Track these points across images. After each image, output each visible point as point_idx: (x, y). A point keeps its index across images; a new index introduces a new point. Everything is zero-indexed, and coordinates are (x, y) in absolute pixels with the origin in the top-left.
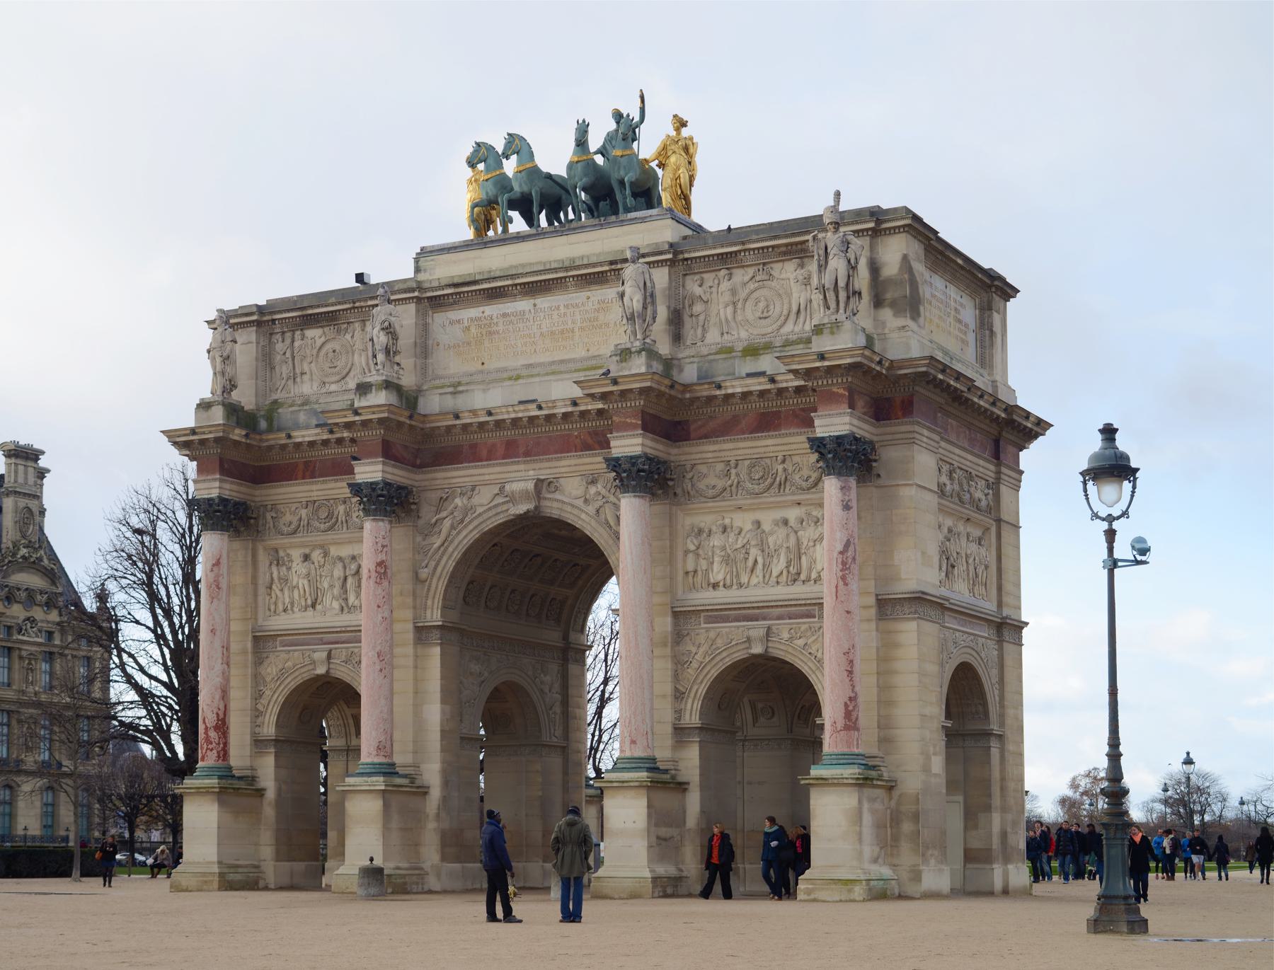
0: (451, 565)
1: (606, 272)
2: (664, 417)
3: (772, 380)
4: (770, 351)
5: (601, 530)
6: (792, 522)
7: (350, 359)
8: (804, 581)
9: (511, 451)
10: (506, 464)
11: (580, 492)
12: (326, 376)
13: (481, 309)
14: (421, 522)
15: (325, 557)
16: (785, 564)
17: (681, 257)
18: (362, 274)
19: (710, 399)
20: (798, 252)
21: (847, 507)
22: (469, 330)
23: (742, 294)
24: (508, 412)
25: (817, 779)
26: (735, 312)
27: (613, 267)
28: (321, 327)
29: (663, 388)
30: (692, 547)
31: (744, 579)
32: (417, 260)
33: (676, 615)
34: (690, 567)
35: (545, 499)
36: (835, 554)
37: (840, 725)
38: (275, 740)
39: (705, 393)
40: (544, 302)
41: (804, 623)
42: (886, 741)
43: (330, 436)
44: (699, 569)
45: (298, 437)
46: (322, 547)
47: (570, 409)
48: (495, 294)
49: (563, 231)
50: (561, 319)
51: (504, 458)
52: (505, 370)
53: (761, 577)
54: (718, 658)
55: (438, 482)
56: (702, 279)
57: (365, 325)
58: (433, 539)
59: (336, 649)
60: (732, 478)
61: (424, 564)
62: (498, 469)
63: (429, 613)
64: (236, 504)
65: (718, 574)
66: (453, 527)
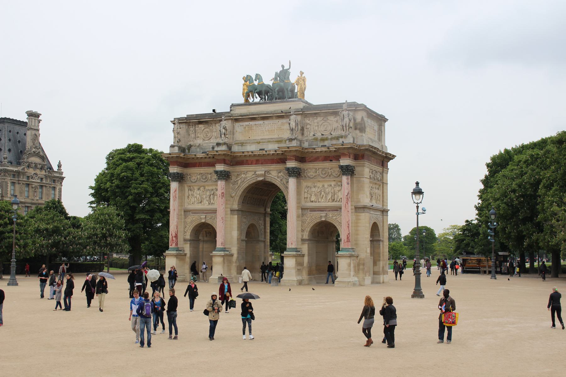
0: (240, 193)
1: (284, 115)
2: (300, 156)
3: (328, 148)
5: (282, 185)
6: (332, 186)
9: (257, 162)
10: (256, 166)
11: (276, 175)
12: (205, 138)
13: (249, 122)
14: (232, 181)
17: (304, 113)
18: (215, 110)
19: (312, 152)
20: (335, 114)
21: (348, 184)
23: (320, 123)
24: (257, 153)
25: (340, 255)
26: (318, 128)
27: (286, 114)
28: (204, 124)
29: (300, 150)
30: (306, 191)
32: (231, 107)
33: (302, 209)
34: (306, 197)
35: (267, 176)
36: (345, 196)
37: (346, 241)
38: (190, 240)
39: (311, 151)
40: (266, 122)
42: (356, 244)
43: (207, 156)
44: (308, 197)
45: (198, 156)
46: (203, 186)
47: (274, 153)
48: (253, 119)
49: (271, 103)
51: (256, 164)
52: (256, 140)
53: (324, 199)
54: (313, 221)
55: (237, 170)
56: (309, 119)
57: (216, 125)
58: (236, 186)
59: (208, 215)
60: (317, 173)
61: (233, 193)
63: (234, 206)
64: (181, 174)
65: (313, 198)
66: (241, 183)
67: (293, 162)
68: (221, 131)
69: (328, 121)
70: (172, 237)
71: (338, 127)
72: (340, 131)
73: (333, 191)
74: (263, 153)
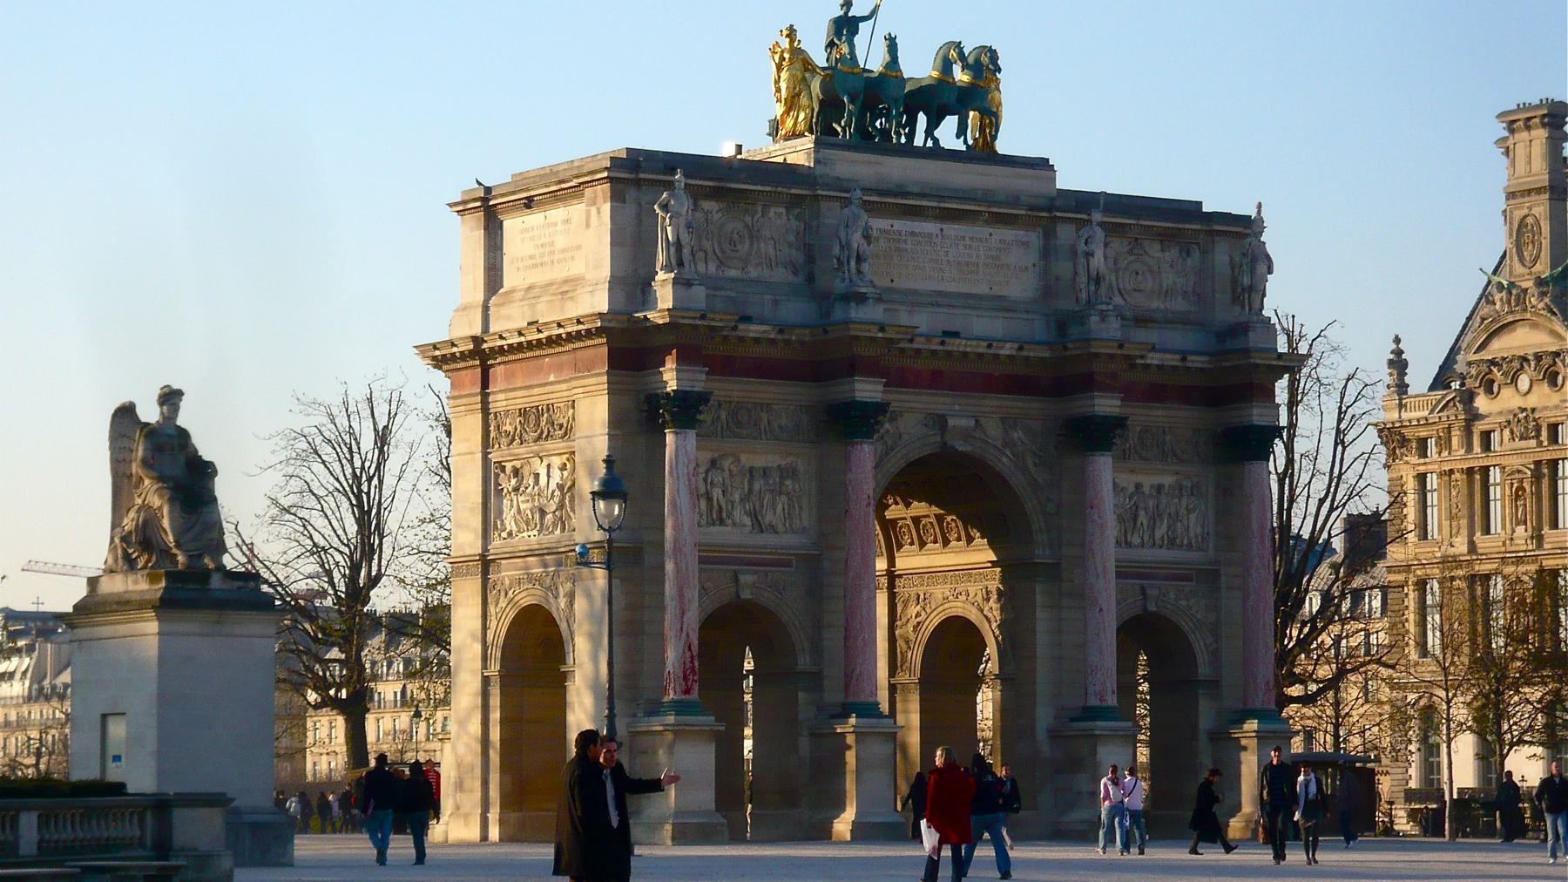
3: (1184, 359)
4: (1156, 325)
7: (755, 246)
8: (1178, 546)
9: (935, 381)
13: (890, 222)
15: (736, 466)
16: (1166, 530)
22: (878, 241)
26: (1117, 279)
27: (1029, 213)
31: (1129, 540)
40: (952, 229)
41: (1185, 586)
47: (1014, 353)
50: (967, 251)
51: (930, 387)
52: (915, 292)
62: (924, 398)
67: (1112, 398)
68: (855, 246)
69: (1147, 259)
70: (692, 657)
71: (1175, 283)
72: (1180, 299)
73: (1173, 510)
74: (975, 350)
